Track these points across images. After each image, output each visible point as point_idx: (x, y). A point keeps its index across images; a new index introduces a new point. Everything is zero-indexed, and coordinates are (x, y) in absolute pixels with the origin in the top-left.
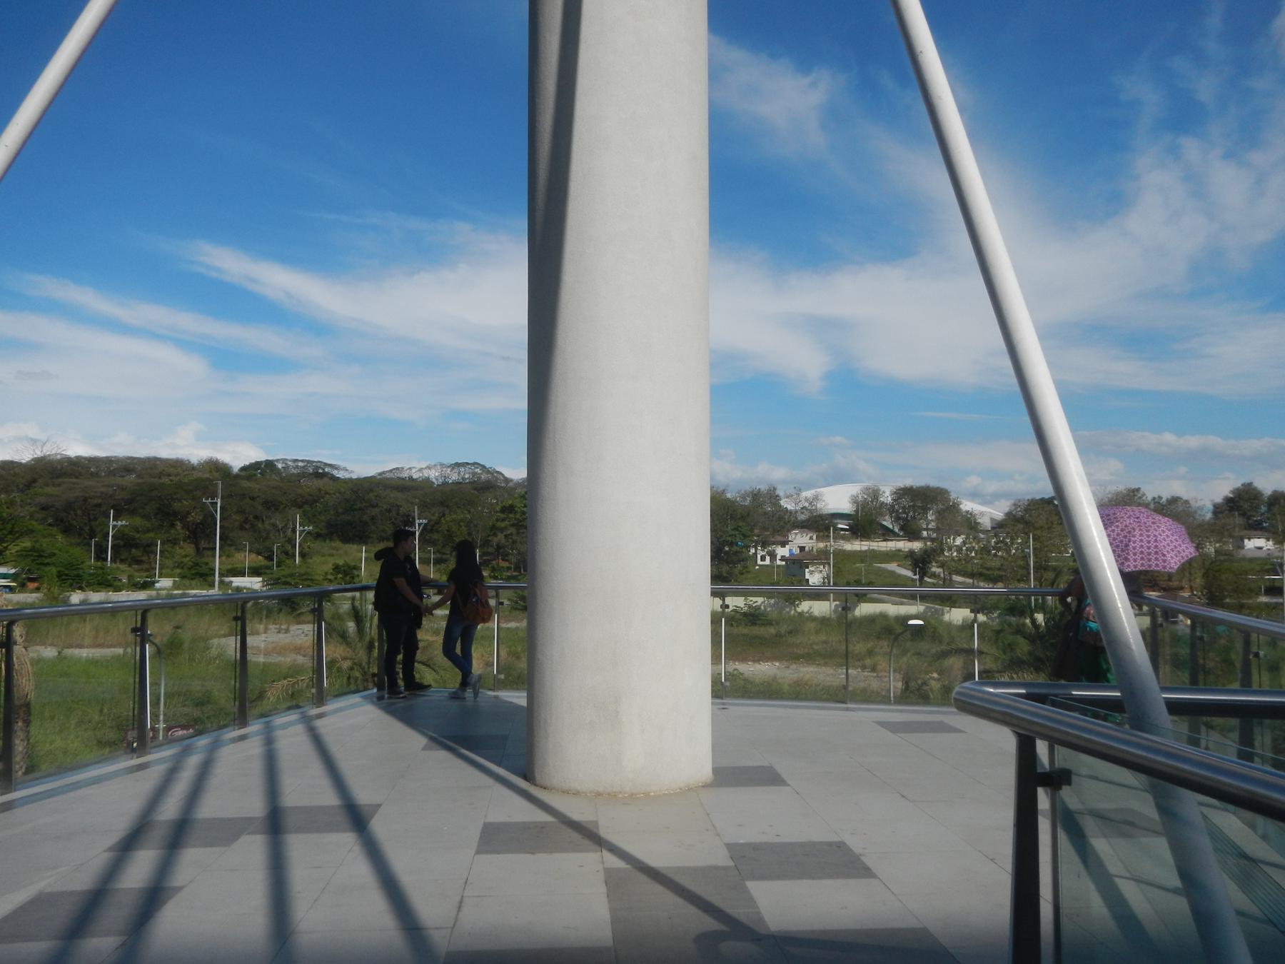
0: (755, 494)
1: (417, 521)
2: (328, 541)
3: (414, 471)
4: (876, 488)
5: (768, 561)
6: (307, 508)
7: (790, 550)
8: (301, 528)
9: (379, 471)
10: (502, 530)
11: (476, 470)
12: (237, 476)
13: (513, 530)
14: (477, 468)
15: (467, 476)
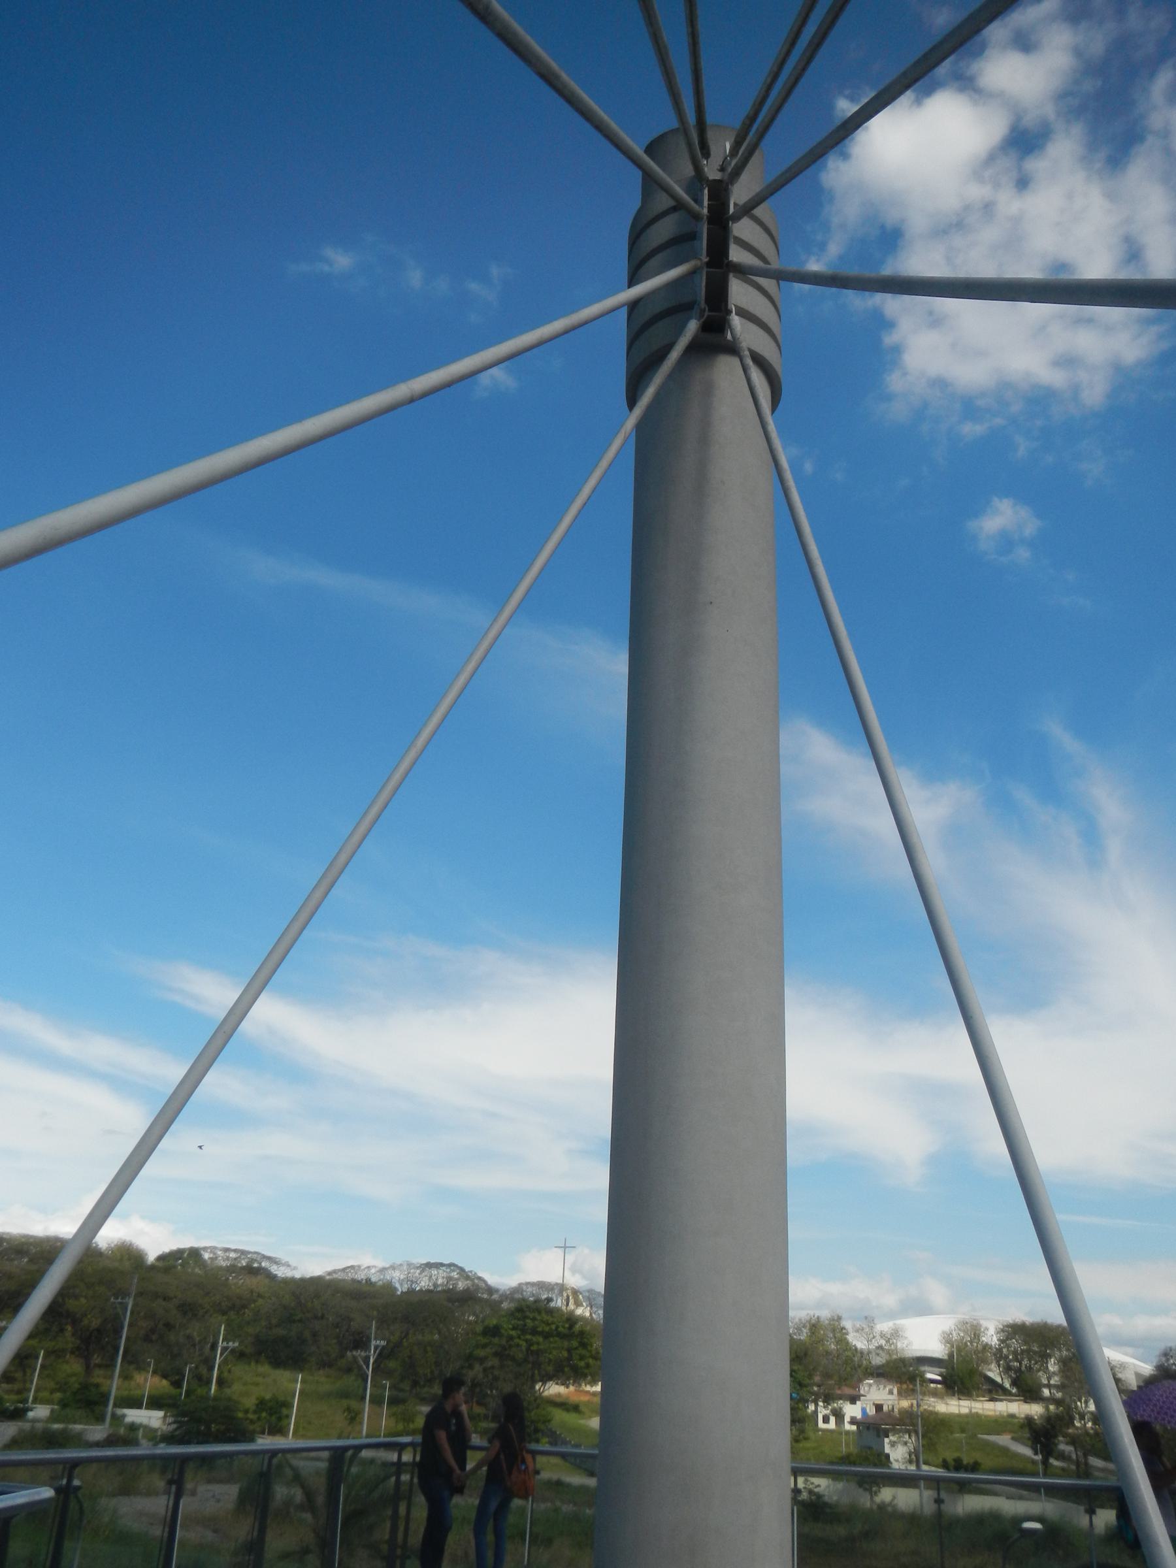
0: (814, 1325)
1: (373, 1343)
2: (253, 1364)
3: (373, 1271)
4: (975, 1322)
5: (832, 1424)
7: (864, 1410)
8: (225, 1344)
9: (329, 1269)
10: (482, 1360)
11: (452, 1274)
12: (153, 1267)
13: (495, 1362)
14: (454, 1271)
15: (440, 1281)
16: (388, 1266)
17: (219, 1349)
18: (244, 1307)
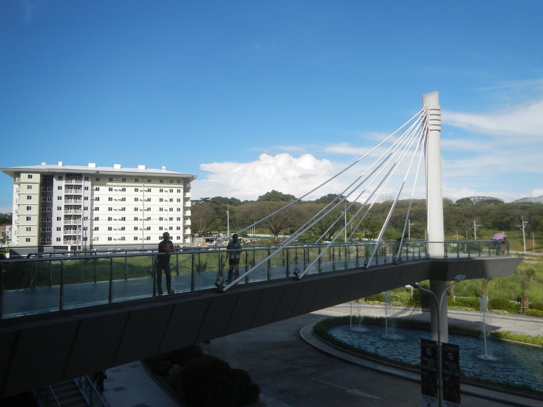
1: (523, 222)
3: (532, 199)
6: (484, 216)
8: (476, 225)
17: (475, 227)
18: (488, 213)
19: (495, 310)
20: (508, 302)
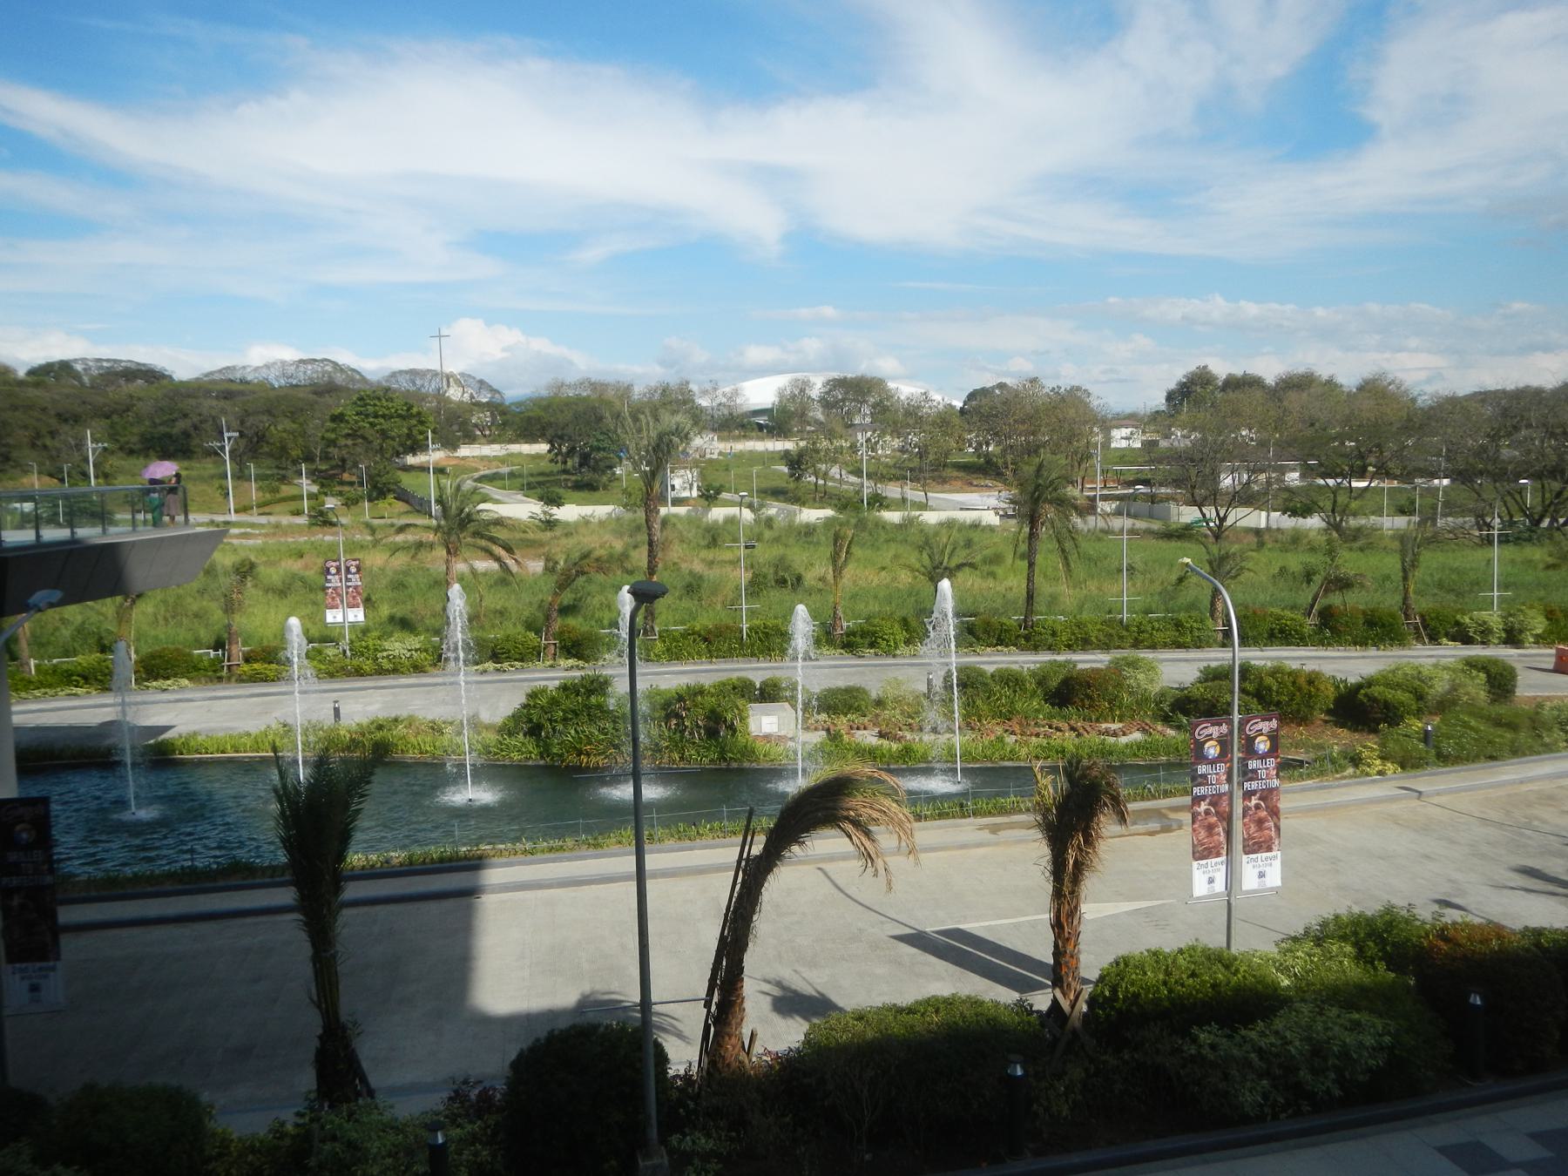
1: (226, 435)
3: (249, 370)
6: (115, 418)
8: (94, 445)
16: (261, 365)
18: (128, 410)
19: (154, 683)
20: (190, 655)
